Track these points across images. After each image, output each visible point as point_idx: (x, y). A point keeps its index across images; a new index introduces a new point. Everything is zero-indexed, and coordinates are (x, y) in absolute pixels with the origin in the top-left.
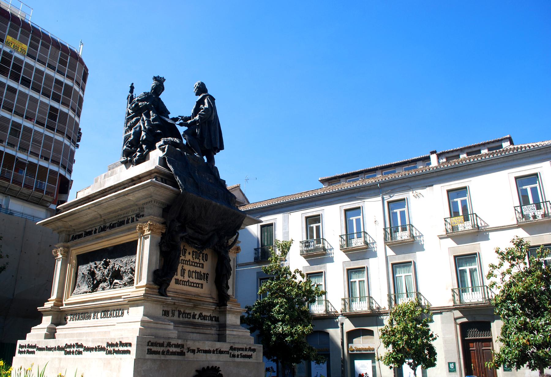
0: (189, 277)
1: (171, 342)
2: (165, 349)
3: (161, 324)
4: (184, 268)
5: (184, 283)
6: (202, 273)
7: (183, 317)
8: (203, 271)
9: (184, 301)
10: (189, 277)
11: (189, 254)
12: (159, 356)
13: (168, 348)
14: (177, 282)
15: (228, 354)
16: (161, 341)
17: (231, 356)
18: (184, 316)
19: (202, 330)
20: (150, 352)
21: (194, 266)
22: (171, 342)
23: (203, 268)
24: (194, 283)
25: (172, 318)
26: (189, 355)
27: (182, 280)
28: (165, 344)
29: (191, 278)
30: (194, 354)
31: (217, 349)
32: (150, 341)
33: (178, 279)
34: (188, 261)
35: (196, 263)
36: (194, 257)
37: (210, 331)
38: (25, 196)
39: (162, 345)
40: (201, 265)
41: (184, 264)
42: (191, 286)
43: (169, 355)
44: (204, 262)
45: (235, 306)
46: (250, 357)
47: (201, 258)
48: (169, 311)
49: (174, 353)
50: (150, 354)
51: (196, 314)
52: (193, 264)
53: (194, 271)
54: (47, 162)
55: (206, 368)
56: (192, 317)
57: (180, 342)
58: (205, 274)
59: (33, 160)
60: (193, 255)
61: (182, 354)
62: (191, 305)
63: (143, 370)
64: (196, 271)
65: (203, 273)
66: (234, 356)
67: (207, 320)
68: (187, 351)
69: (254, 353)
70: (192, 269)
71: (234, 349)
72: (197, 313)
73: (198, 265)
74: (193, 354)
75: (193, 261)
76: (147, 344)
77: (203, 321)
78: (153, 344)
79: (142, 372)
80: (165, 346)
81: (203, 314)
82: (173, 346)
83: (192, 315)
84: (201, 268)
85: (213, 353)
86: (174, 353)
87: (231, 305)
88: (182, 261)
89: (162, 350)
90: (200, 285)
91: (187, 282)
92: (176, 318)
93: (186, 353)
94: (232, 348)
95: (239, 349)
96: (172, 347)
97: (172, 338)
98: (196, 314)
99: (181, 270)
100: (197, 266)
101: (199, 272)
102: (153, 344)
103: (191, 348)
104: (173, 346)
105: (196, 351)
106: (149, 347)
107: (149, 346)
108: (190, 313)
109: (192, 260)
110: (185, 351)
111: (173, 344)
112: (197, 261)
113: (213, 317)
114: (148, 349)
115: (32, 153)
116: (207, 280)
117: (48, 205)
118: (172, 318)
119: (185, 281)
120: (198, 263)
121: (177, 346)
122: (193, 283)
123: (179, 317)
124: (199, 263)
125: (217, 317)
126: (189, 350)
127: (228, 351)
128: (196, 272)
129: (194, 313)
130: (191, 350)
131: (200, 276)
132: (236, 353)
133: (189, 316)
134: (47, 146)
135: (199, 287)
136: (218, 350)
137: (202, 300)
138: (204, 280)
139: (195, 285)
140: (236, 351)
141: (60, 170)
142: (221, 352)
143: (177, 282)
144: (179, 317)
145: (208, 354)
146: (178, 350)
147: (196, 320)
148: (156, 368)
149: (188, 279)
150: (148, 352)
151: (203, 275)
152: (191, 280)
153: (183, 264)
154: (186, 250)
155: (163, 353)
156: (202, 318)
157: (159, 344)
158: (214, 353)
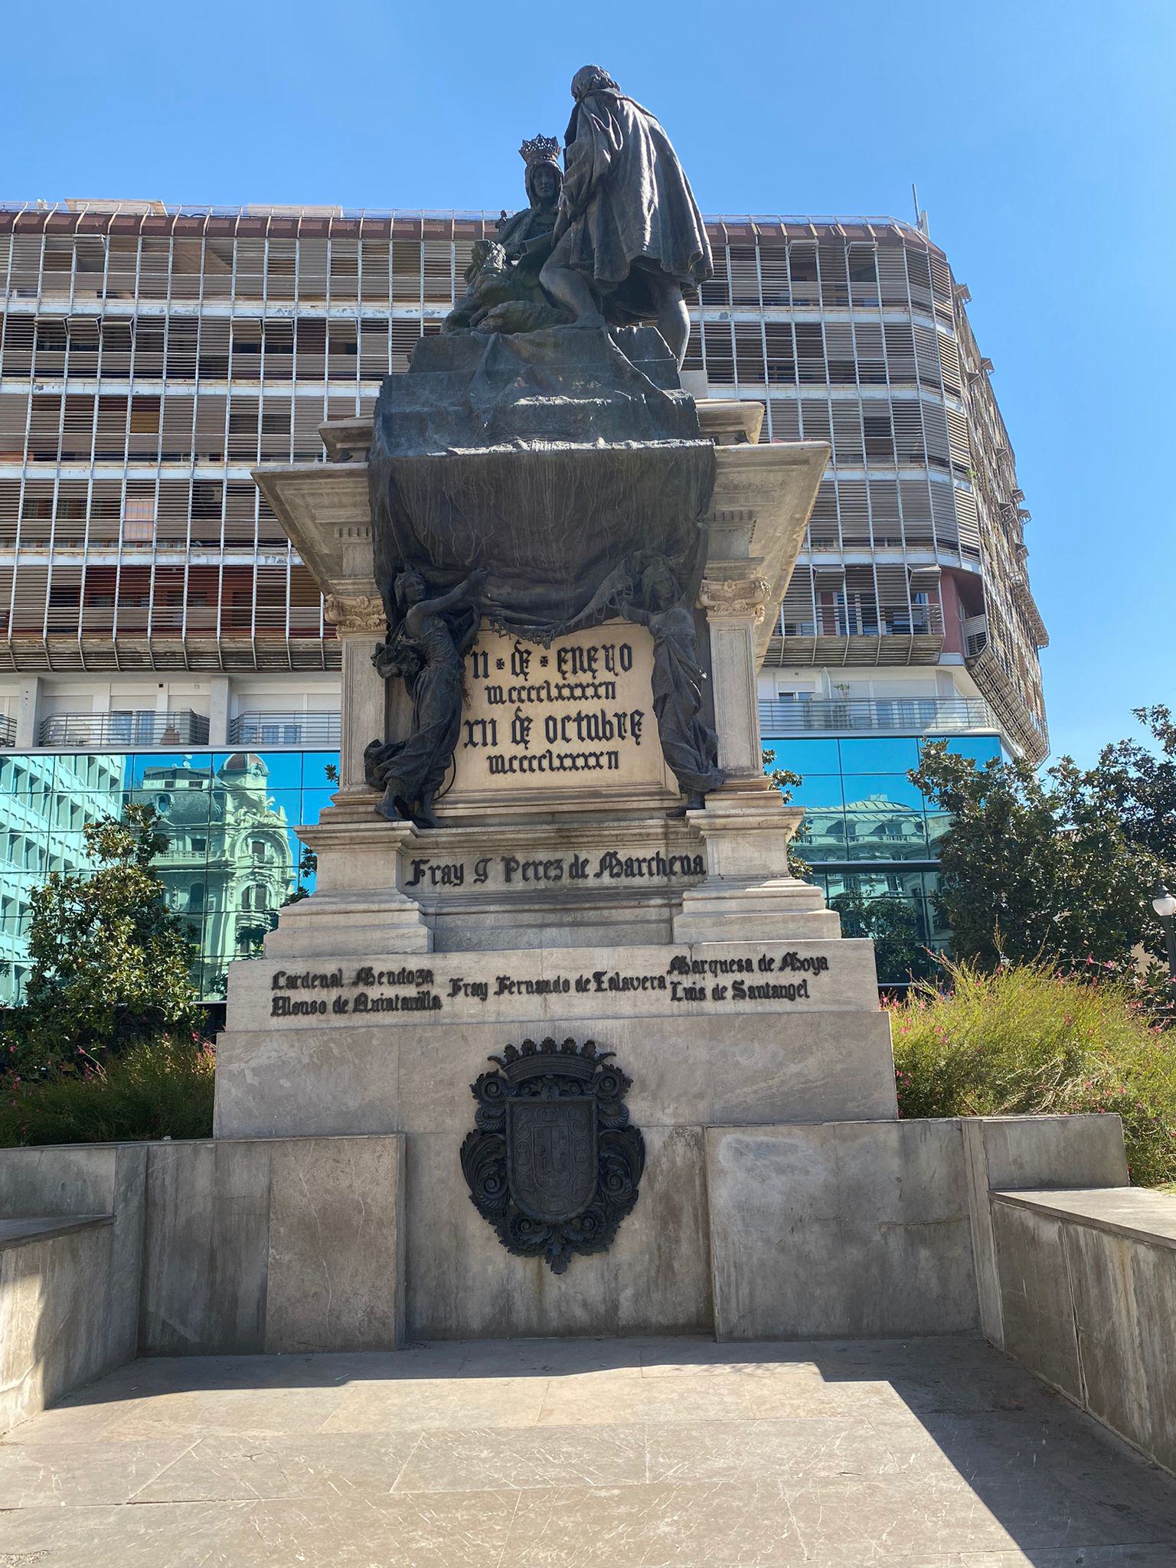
0: (551, 741)
1: (371, 969)
2: (349, 994)
3: (365, 912)
4: (522, 715)
5: (527, 764)
6: (610, 717)
7: (525, 878)
8: (611, 708)
9: (527, 824)
10: (551, 741)
11: (544, 661)
12: (322, 1017)
13: (362, 989)
14: (497, 765)
15: (662, 986)
16: (329, 968)
17: (680, 993)
18: (530, 872)
19: (592, 913)
20: (281, 1007)
21: (573, 697)
22: (371, 969)
23: (614, 697)
24: (574, 758)
25: (479, 888)
26: (466, 1006)
27: (519, 756)
28: (349, 975)
29: (559, 741)
30: (484, 999)
31: (598, 976)
32: (283, 974)
33: (501, 756)
34: (538, 690)
35: (580, 685)
36: (568, 667)
37: (638, 911)
38: (865, 656)
39: (335, 981)
40: (602, 691)
41: (522, 701)
42: (562, 767)
43: (367, 1011)
44: (617, 675)
45: (755, 803)
46: (790, 993)
47: (599, 665)
48: (462, 866)
49: (389, 1005)
50: (284, 1014)
51: (586, 861)
52: (566, 692)
53: (574, 715)
54: (896, 549)
55: (580, 1044)
56: (566, 874)
57: (414, 964)
58: (625, 715)
59: (858, 557)
60: (561, 661)
61: (427, 1003)
62: (544, 831)
63: (253, 1069)
64: (579, 713)
65: (616, 715)
66: (695, 994)
67: (641, 875)
68: (450, 990)
69: (816, 974)
70: (560, 709)
71: (698, 967)
72: (594, 857)
73: (590, 691)
74: (476, 999)
75: (561, 682)
76: (270, 982)
77: (624, 881)
78: (292, 982)
79: (248, 1074)
80: (345, 981)
81: (622, 856)
82: (385, 980)
83: (566, 867)
84: (603, 699)
85: (578, 990)
86: (389, 1005)
87: (729, 802)
88: (515, 695)
89: (334, 998)
90: (604, 760)
91: (544, 756)
92: (495, 884)
93: (445, 1000)
94: (678, 965)
95: (726, 966)
96: (381, 983)
97: (405, 953)
98: (586, 861)
99: (514, 723)
100: (584, 696)
101: (595, 716)
102: (292, 982)
103: (470, 980)
104: (385, 980)
105: (493, 988)
106: (280, 993)
107: (281, 988)
108: (559, 861)
109: (556, 678)
110: (439, 989)
111: (381, 975)
112: (585, 678)
113: (674, 857)
114: (275, 1000)
115: (848, 542)
116: (637, 737)
117: (935, 659)
118: (479, 888)
119: (534, 757)
120: (588, 685)
121: (403, 977)
122: (571, 756)
123: (508, 879)
124: (593, 685)
125: (692, 858)
126: (456, 986)
127: (662, 979)
128: (579, 719)
129: (576, 857)
130: (466, 986)
131: (598, 727)
132: (709, 982)
133: (553, 873)
134: (885, 510)
135: (599, 765)
136: (605, 979)
137: (607, 806)
138: (623, 738)
139: (580, 762)
140: (709, 975)
141: (939, 556)
142: (620, 984)
143: (497, 765)
144: (508, 879)
145: (553, 998)
146: (410, 991)
147: (591, 882)
148: (306, 1060)
149: (548, 746)
150: (276, 1007)
151: (615, 721)
152: (559, 747)
153: (517, 704)
154: (529, 653)
155: (340, 1007)
156: (615, 871)
157: (323, 978)
158: (582, 986)
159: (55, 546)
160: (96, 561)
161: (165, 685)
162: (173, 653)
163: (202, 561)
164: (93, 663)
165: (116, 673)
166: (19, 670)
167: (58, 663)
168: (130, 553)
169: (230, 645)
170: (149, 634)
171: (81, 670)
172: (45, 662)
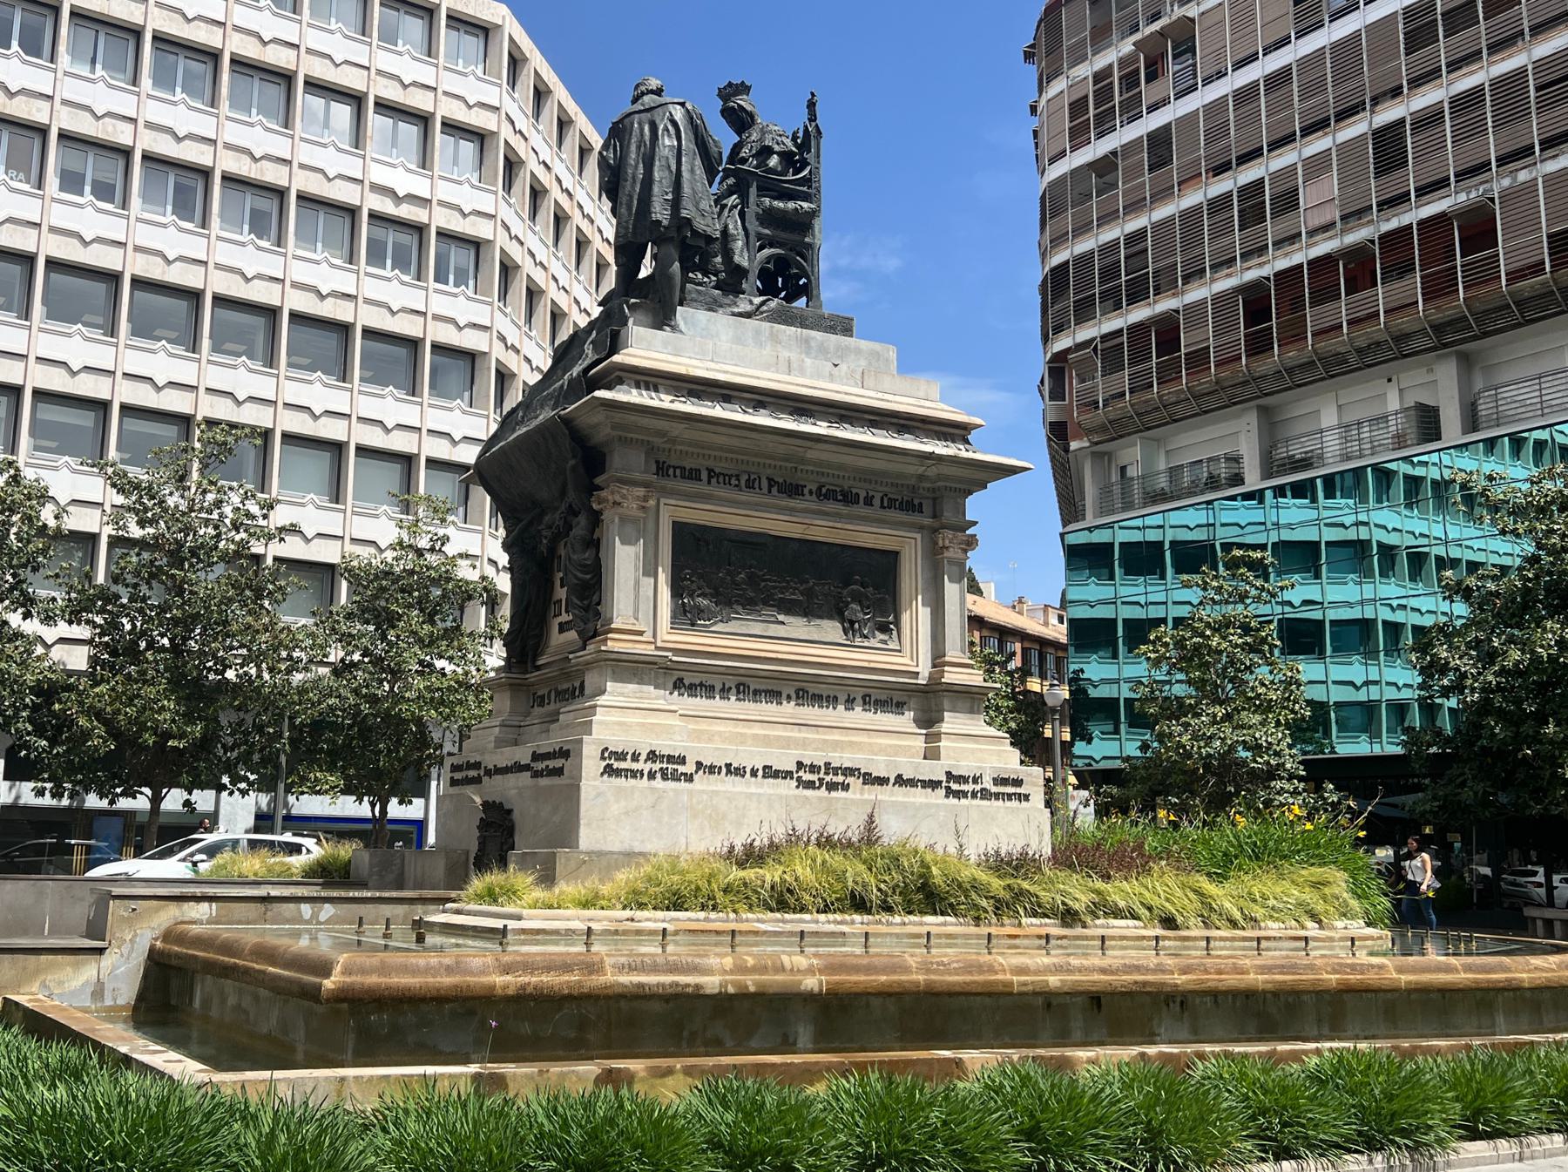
159: (1242, 262)
160: (1283, 264)
161: (1394, 378)
162: (1378, 344)
163: (1394, 224)
164: (1300, 377)
165: (1327, 382)
166: (1234, 404)
167: (1266, 386)
168: (1315, 244)
169: (1437, 317)
170: (1345, 331)
171: (1290, 388)
172: (1252, 389)
